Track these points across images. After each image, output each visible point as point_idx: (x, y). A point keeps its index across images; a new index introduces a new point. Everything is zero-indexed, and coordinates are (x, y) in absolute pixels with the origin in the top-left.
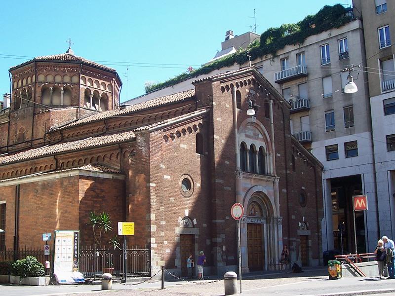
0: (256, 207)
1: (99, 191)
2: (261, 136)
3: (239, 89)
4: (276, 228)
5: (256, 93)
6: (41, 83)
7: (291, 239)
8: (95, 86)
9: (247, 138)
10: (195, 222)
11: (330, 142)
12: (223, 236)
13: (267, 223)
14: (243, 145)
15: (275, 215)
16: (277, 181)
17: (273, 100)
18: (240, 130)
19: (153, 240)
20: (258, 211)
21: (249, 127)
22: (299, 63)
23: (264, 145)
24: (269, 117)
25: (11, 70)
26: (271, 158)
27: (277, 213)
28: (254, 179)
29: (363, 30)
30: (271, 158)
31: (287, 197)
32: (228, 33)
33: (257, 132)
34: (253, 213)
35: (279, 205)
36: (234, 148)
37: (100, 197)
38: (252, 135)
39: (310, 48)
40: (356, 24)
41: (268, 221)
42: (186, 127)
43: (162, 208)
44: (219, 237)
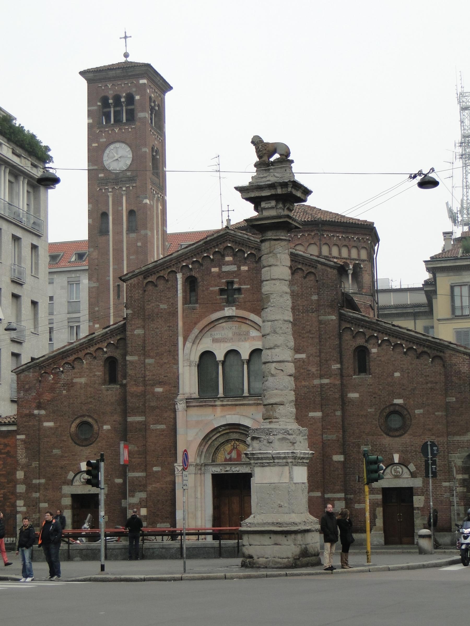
1: (2, 446)
2: (254, 333)
3: (193, 274)
5: (239, 267)
9: (218, 344)
12: (143, 495)
14: (207, 355)
18: (192, 336)
19: (20, 503)
21: (224, 324)
28: (222, 405)
33: (244, 328)
34: (236, 457)
37: (4, 453)
38: (230, 335)
42: (81, 355)
43: (35, 464)
44: (133, 496)
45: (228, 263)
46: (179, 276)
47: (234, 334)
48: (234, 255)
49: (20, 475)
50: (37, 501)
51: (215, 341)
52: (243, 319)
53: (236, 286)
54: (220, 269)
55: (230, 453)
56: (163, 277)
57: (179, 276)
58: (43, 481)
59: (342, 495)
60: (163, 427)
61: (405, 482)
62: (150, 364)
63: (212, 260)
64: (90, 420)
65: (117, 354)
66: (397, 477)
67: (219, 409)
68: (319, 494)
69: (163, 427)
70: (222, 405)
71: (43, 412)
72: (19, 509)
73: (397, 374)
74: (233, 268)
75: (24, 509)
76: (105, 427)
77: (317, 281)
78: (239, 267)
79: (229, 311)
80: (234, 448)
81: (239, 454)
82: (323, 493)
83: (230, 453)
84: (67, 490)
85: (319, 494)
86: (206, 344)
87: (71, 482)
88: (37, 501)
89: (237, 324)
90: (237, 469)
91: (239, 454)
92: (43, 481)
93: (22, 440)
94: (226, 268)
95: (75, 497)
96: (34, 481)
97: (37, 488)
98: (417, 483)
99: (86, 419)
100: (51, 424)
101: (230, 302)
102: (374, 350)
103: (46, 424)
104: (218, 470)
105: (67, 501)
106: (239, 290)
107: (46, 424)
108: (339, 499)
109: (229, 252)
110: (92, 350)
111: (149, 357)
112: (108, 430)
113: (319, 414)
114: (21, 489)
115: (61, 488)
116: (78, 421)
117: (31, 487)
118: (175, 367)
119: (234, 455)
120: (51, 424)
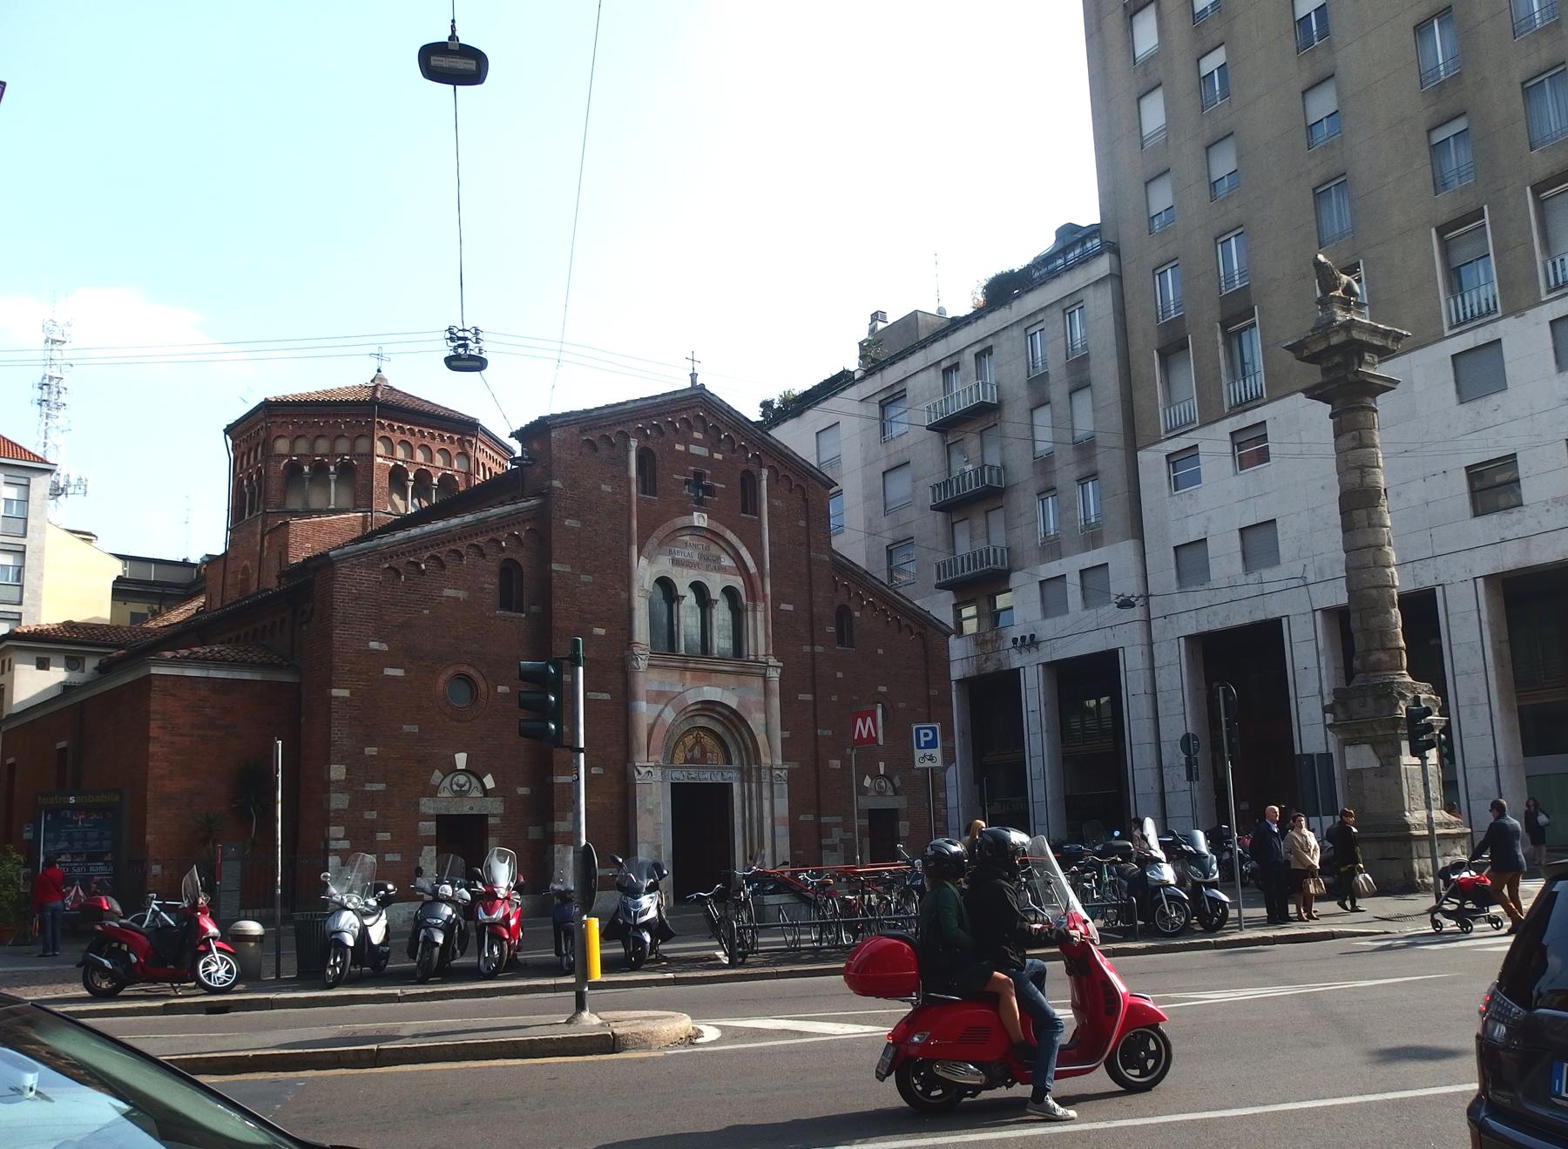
0: (708, 741)
2: (727, 561)
3: (650, 445)
4: (766, 793)
6: (283, 456)
7: (824, 820)
8: (420, 456)
10: (489, 782)
11: (1050, 569)
13: (742, 781)
15: (765, 760)
16: (774, 675)
17: (770, 467)
19: (336, 831)
20: (717, 750)
21: (687, 538)
22: (980, 374)
23: (738, 582)
24: (756, 510)
25: (229, 430)
26: (760, 616)
27: (772, 756)
28: (693, 670)
29: (1120, 278)
30: (760, 616)
31: (815, 715)
32: (876, 317)
33: (714, 550)
35: (778, 735)
36: (624, 595)
38: (696, 558)
39: (1003, 336)
40: (1103, 266)
41: (745, 776)
42: (462, 546)
44: (563, 819)
45: (697, 442)
46: (634, 443)
47: (701, 556)
48: (705, 432)
49: (337, 772)
50: (373, 828)
51: (676, 562)
52: (711, 535)
53: (707, 482)
54: (687, 449)
55: (691, 750)
56: (608, 438)
57: (634, 443)
58: (381, 787)
59: (840, 819)
60: (606, 696)
61: (890, 802)
62: (585, 584)
63: (676, 430)
64: (472, 672)
65: (521, 557)
66: (881, 793)
67: (688, 675)
68: (810, 818)
69: (606, 696)
70: (693, 670)
71: (385, 647)
72: (333, 845)
73: (880, 651)
74: (702, 451)
75: (345, 844)
76: (500, 689)
77: (806, 500)
78: (711, 455)
79: (700, 519)
80: (698, 741)
81: (704, 752)
82: (818, 816)
83: (691, 750)
84: (428, 806)
85: (810, 818)
86: (663, 566)
87: (432, 792)
88: (373, 828)
89: (704, 543)
90: (707, 775)
91: (704, 752)
92: (381, 787)
93: (343, 700)
94: (694, 449)
95: (442, 820)
96: (369, 787)
97: (371, 800)
98: (899, 803)
99: (465, 669)
100: (399, 672)
101: (700, 504)
102: (857, 614)
103: (389, 672)
104: (681, 776)
105: (428, 828)
106: (709, 490)
107: (389, 672)
108: (837, 825)
109: (700, 425)
110: (480, 540)
111: (585, 571)
112: (506, 695)
113: (809, 697)
114: (339, 801)
115: (418, 803)
116: (450, 672)
117: (363, 800)
118: (624, 595)
119: (697, 752)
120: (399, 672)
